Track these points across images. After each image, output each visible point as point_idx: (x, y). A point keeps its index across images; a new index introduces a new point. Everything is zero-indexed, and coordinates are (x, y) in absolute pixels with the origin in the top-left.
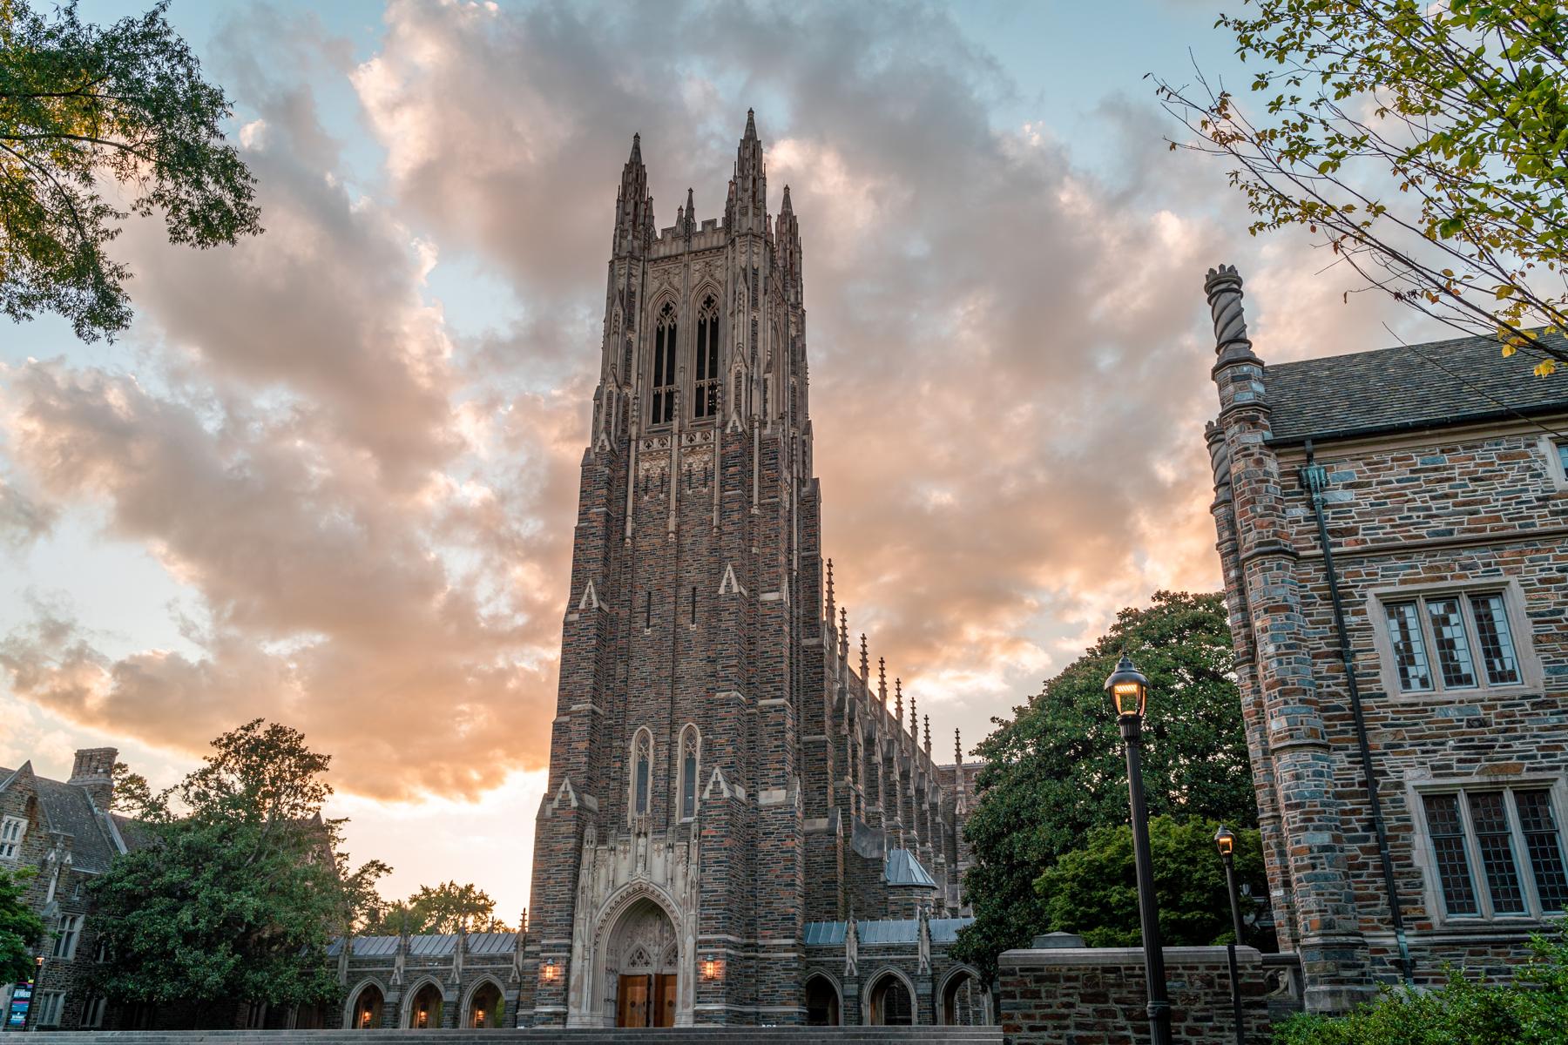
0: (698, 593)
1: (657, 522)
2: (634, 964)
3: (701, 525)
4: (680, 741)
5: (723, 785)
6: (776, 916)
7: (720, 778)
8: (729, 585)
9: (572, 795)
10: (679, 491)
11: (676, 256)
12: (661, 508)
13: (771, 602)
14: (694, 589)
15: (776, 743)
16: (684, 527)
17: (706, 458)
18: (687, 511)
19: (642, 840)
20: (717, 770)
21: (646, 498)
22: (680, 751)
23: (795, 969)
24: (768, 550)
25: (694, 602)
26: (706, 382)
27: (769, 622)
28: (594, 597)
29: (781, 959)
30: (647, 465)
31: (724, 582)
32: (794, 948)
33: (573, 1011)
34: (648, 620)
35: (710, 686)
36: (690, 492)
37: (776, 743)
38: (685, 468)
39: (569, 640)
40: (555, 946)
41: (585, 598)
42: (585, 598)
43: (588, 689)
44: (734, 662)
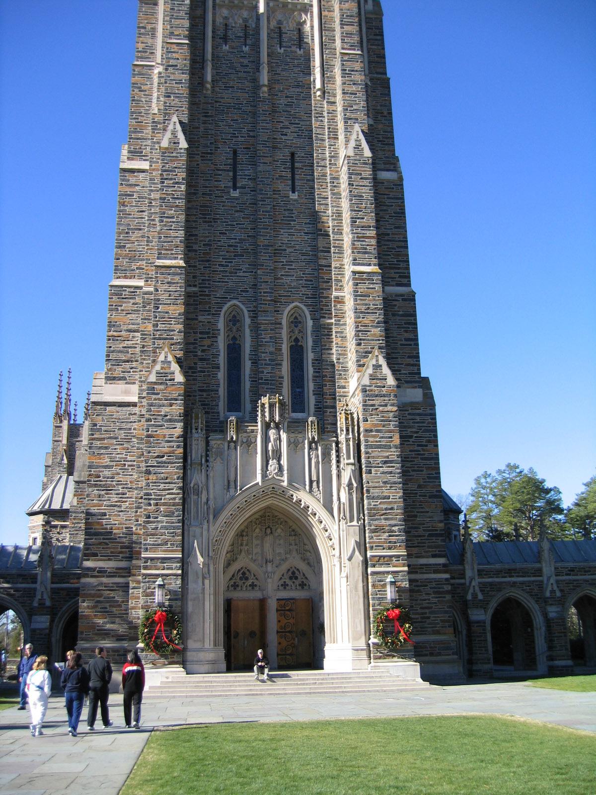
0: (297, 159)
1: (240, 75)
2: (235, 586)
3: (298, 86)
4: (284, 322)
5: (386, 370)
6: (421, 532)
7: (382, 362)
9: (175, 367)
12: (245, 62)
13: (388, 181)
14: (293, 155)
15: (407, 335)
16: (277, 87)
18: (279, 70)
21: (226, 48)
22: (284, 333)
23: (448, 592)
24: (380, 126)
25: (293, 169)
27: (387, 202)
29: (430, 581)
30: (225, 12)
32: (445, 568)
33: (191, 644)
37: (407, 335)
38: (273, 24)
39: (128, 190)
40: (164, 560)
41: (168, 135)
42: (168, 135)
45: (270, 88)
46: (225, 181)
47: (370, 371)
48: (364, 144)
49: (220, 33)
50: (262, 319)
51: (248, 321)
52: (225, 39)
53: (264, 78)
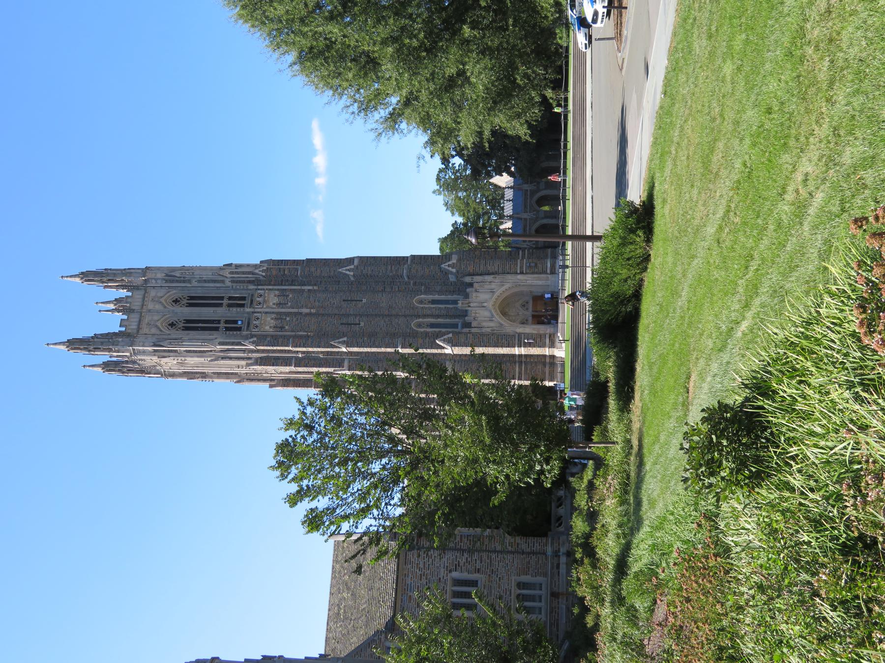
3: (309, 298)
4: (422, 306)
5: (450, 263)
7: (447, 264)
8: (349, 270)
9: (446, 337)
10: (287, 308)
11: (141, 316)
17: (272, 296)
19: (472, 305)
20: (443, 266)
21: (287, 327)
22: (426, 306)
26: (225, 302)
28: (341, 340)
31: (348, 272)
34: (356, 324)
35: (397, 289)
36: (289, 304)
38: (274, 306)
43: (390, 341)
44: (390, 267)
45: (311, 308)
46: (357, 328)
47: (450, 269)
48: (348, 268)
49: (278, 330)
50: (420, 314)
51: (421, 320)
52: (282, 328)
53: (305, 311)
